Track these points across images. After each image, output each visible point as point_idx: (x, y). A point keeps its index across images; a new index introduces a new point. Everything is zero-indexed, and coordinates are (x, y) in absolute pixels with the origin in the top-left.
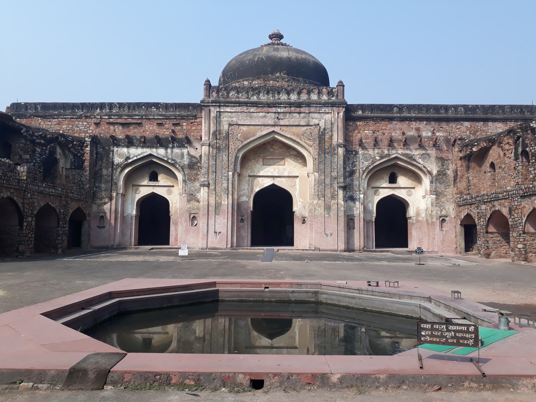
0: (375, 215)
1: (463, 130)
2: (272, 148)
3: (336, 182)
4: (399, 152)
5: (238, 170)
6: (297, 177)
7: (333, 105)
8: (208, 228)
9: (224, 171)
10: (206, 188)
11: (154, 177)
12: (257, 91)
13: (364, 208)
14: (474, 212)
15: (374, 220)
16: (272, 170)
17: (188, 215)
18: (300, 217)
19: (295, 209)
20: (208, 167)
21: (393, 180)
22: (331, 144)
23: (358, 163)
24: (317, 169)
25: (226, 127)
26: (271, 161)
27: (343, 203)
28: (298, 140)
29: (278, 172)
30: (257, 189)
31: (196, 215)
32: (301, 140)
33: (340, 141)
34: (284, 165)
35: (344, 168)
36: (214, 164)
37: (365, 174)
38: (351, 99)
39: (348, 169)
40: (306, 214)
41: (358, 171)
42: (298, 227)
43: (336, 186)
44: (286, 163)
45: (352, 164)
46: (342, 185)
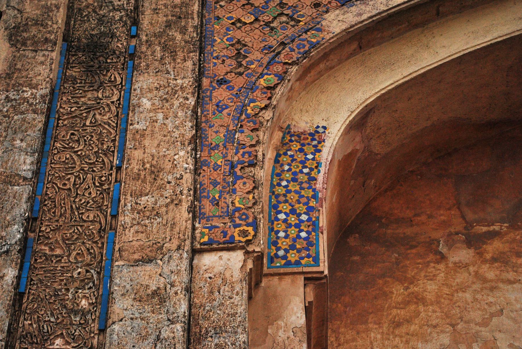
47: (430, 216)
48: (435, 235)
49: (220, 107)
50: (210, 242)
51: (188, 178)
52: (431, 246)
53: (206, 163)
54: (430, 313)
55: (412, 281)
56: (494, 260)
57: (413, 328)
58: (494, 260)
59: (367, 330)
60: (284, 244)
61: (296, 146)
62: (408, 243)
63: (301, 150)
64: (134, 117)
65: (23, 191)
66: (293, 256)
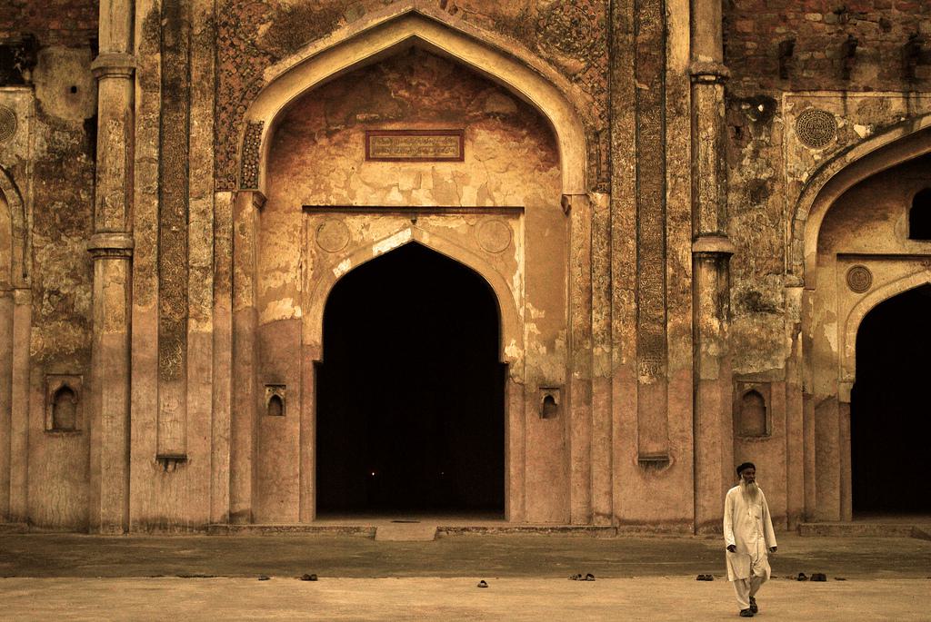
0: (853, 376)
2: (409, 87)
3: (685, 235)
5: (262, 188)
6: (516, 212)
8: (128, 440)
9: (193, 188)
10: (117, 266)
13: (808, 344)
15: (846, 398)
16: (407, 183)
17: (36, 380)
18: (533, 388)
19: (510, 351)
20: (130, 170)
22: (665, 70)
23: (776, 152)
24: (599, 177)
26: (403, 143)
27: (715, 323)
28: (522, 53)
29: (434, 193)
30: (345, 267)
31: (74, 383)
32: (533, 49)
33: (702, 58)
34: (461, 159)
35: (722, 174)
36: (150, 160)
37: (809, 200)
39: (736, 178)
40: (555, 373)
41: (777, 187)
42: (523, 431)
43: (684, 251)
44: (469, 153)
45: (756, 154)
46: (713, 246)
47: (313, 121)
48: (314, 131)
49: (223, 123)
50: (220, 188)
51: (212, 161)
52: (312, 135)
53: (218, 151)
54: (307, 170)
55: (302, 154)
56: (335, 144)
57: (300, 177)
58: (335, 144)
59: (283, 177)
60: (246, 178)
61: (252, 131)
62: (302, 134)
63: (254, 133)
64: (192, 131)
65: (156, 166)
66: (249, 184)
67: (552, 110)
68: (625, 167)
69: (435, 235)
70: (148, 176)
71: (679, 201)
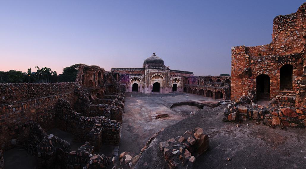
1: (184, 75)
4: (176, 77)
7: (168, 70)
11: (135, 81)
12: (155, 66)
14: (186, 87)
21: (175, 81)
24: (165, 80)
25: (150, 73)
38: (170, 69)
67: (163, 77)
68: (166, 79)
69: (158, 82)
70: (147, 80)
71: (168, 81)
